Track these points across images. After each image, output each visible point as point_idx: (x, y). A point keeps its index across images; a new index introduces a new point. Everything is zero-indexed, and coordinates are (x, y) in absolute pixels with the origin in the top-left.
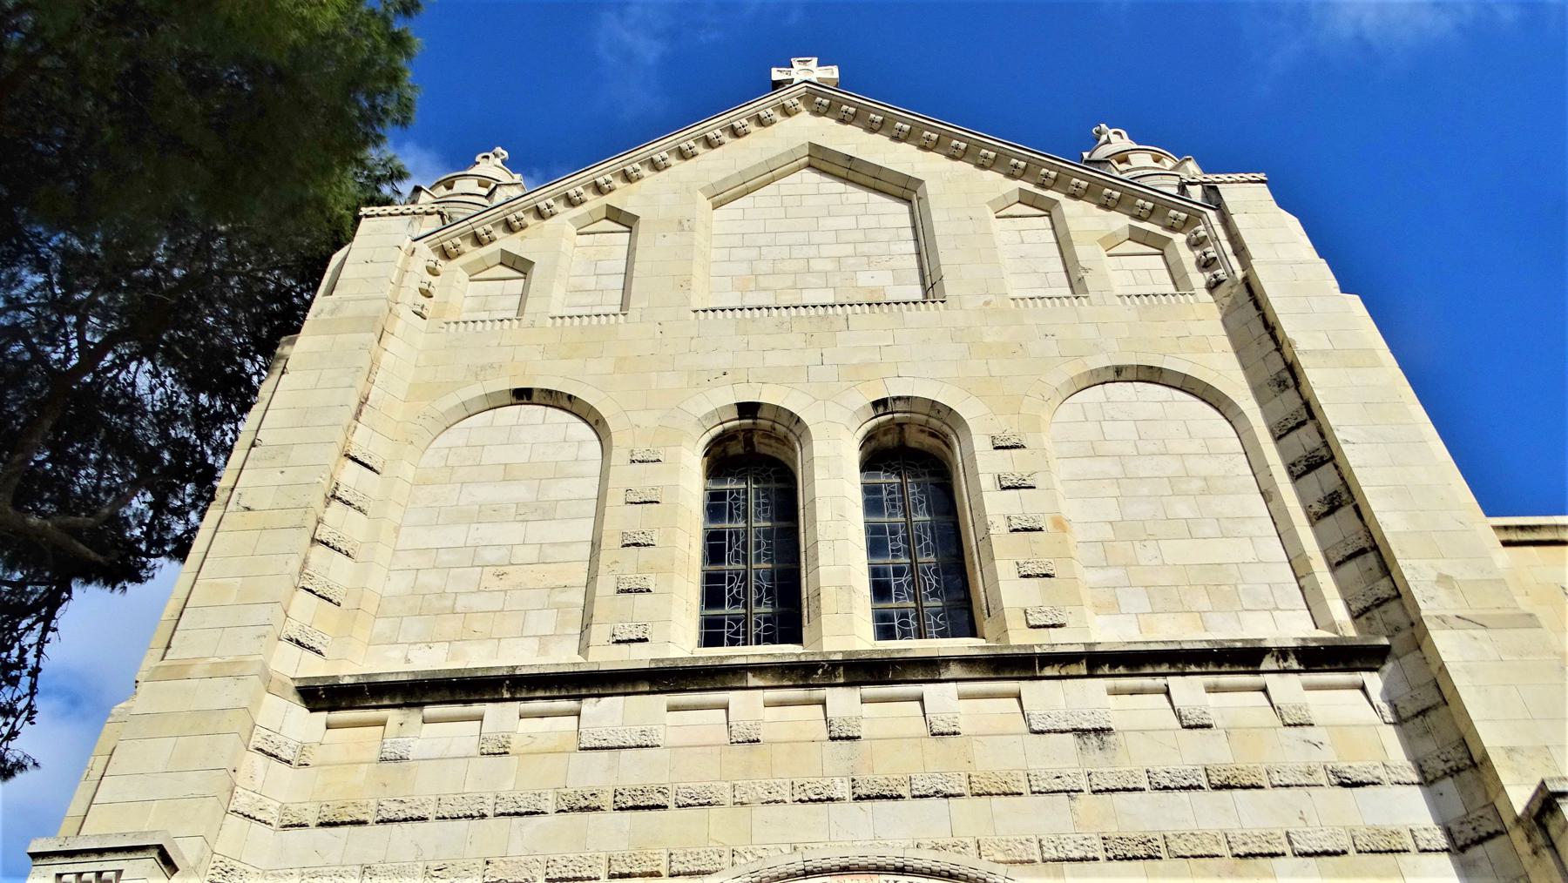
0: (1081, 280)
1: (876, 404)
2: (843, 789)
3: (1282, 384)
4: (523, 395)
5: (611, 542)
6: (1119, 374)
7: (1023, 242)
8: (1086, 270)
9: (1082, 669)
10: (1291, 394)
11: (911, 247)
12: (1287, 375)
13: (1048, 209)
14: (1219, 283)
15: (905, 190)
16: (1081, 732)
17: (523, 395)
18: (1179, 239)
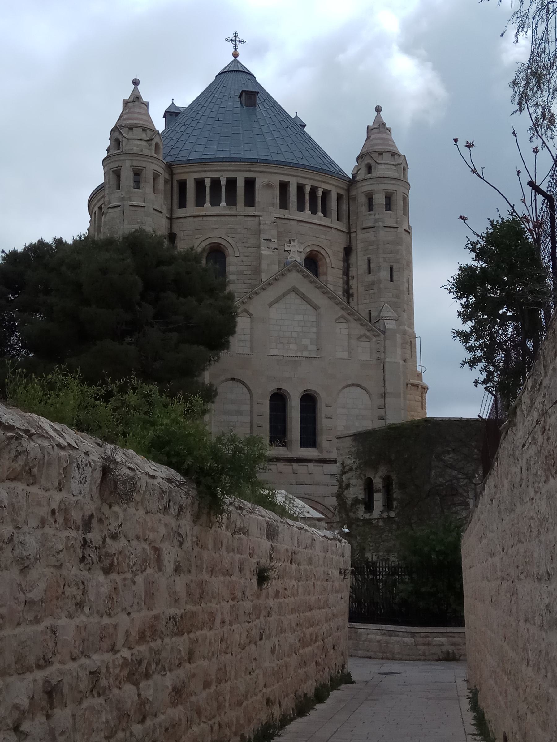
0: (351, 352)
1: (304, 391)
2: (294, 483)
3: (382, 396)
4: (233, 379)
5: (255, 426)
6: (353, 385)
7: (340, 333)
8: (352, 349)
9: (334, 462)
10: (383, 399)
11: (314, 330)
12: (384, 395)
13: (348, 321)
14: (379, 360)
15: (316, 308)
16: (331, 475)
17: (233, 379)
18: (374, 339)
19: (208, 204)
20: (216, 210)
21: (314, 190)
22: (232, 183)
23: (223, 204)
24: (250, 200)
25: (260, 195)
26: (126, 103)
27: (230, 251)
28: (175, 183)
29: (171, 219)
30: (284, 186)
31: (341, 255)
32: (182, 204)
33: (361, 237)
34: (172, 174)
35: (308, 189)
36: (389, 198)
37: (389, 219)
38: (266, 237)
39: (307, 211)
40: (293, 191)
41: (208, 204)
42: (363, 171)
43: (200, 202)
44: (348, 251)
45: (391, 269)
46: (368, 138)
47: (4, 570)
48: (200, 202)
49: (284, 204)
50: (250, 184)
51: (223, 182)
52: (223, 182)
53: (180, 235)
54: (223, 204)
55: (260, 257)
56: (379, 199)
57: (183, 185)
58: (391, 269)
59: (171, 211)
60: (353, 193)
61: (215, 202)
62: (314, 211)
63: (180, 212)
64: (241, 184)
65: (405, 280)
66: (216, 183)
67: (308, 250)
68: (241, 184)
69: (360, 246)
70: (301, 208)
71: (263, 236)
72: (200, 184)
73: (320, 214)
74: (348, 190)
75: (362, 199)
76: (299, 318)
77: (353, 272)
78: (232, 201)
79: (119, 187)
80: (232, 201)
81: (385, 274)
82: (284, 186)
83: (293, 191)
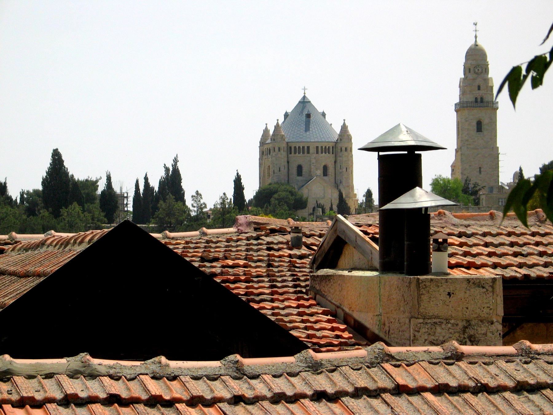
19: (297, 154)
20: (299, 155)
21: (325, 147)
22: (303, 147)
23: (301, 153)
24: (308, 152)
25: (311, 151)
26: (275, 127)
27: (303, 166)
28: (289, 147)
29: (288, 157)
30: (317, 147)
31: (334, 164)
32: (291, 153)
33: (338, 158)
34: (288, 145)
35: (324, 147)
36: (346, 149)
37: (346, 154)
38: (312, 162)
39: (324, 153)
40: (320, 148)
41: (297, 154)
42: (339, 140)
43: (295, 153)
44: (335, 162)
45: (346, 168)
46: (341, 129)
47: (202, 201)
48: (295, 153)
49: (317, 153)
50: (308, 148)
51: (301, 148)
52: (301, 148)
53: (290, 162)
54: (301, 153)
55: (311, 168)
56: (344, 149)
57: (291, 148)
58: (346, 168)
59: (288, 155)
60: (337, 146)
61: (299, 153)
62: (325, 153)
63: (290, 155)
64: (306, 148)
65: (350, 171)
66: (299, 147)
67: (324, 164)
68: (306, 148)
69: (338, 161)
70: (322, 153)
71: (312, 162)
72: (295, 147)
73: (327, 153)
74: (335, 145)
75: (339, 148)
76: (320, 189)
77: (336, 168)
78: (303, 153)
79: (275, 151)
80: (303, 153)
81: (345, 170)
82: (317, 147)
83: (320, 148)
